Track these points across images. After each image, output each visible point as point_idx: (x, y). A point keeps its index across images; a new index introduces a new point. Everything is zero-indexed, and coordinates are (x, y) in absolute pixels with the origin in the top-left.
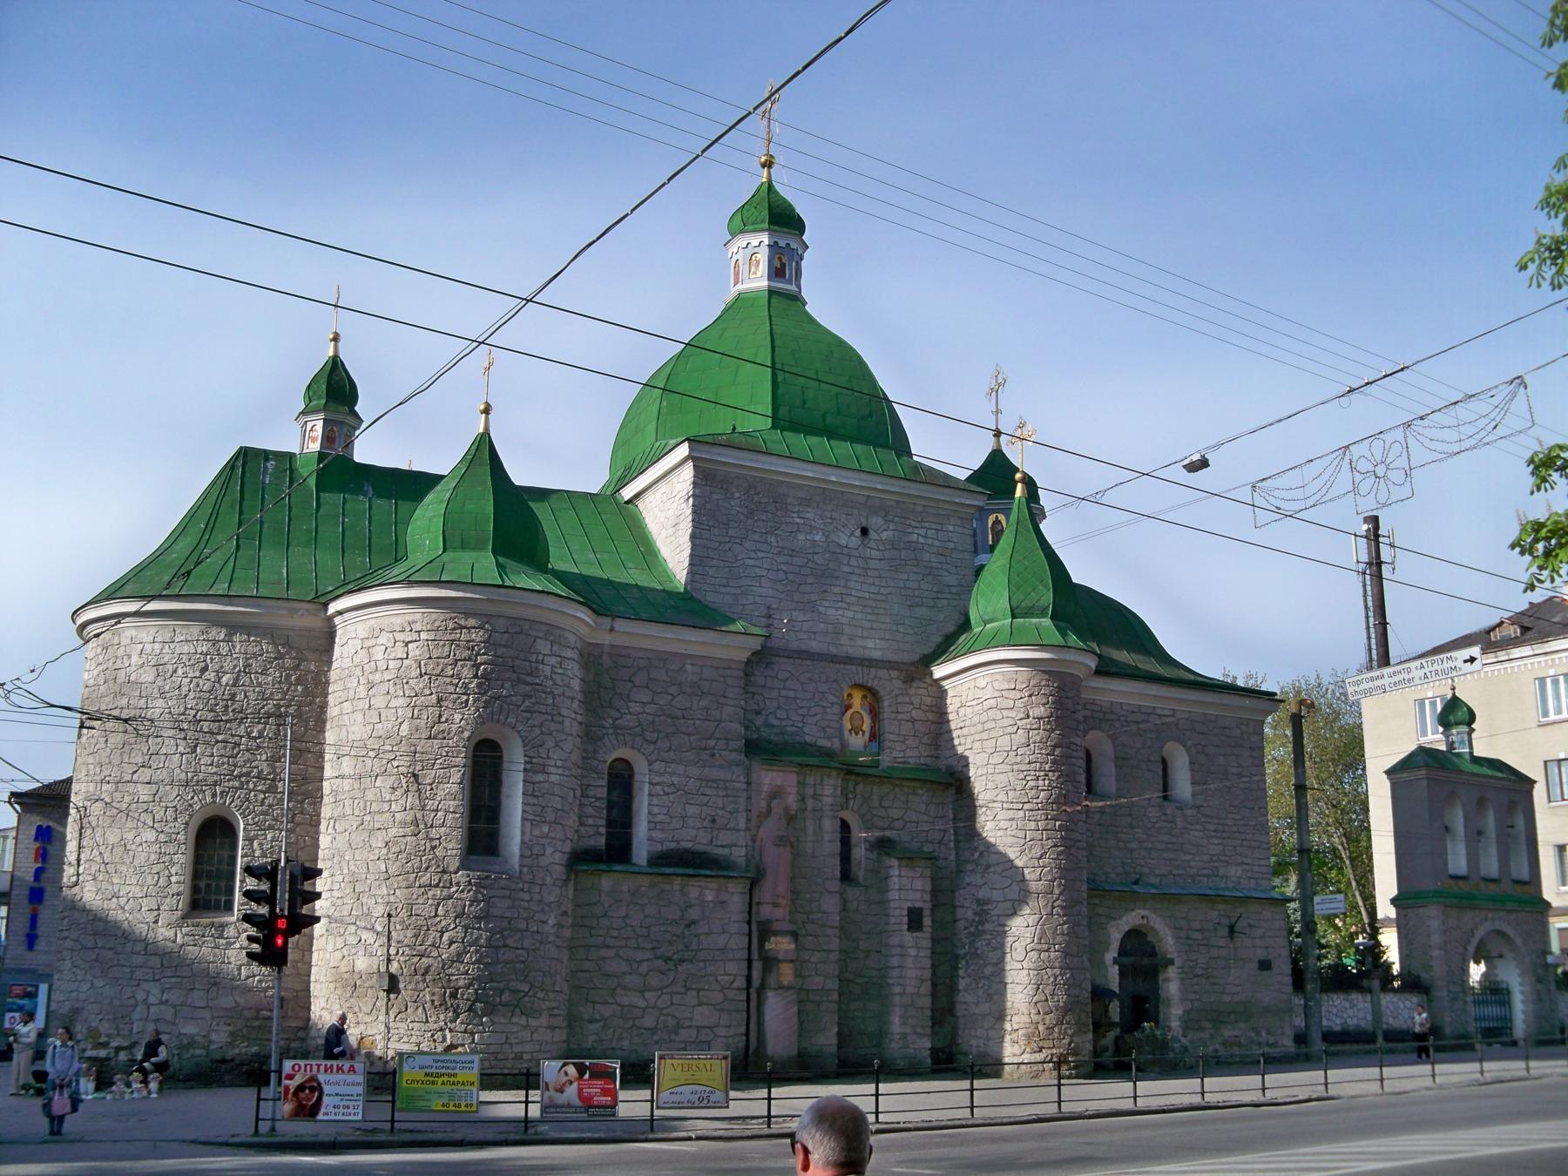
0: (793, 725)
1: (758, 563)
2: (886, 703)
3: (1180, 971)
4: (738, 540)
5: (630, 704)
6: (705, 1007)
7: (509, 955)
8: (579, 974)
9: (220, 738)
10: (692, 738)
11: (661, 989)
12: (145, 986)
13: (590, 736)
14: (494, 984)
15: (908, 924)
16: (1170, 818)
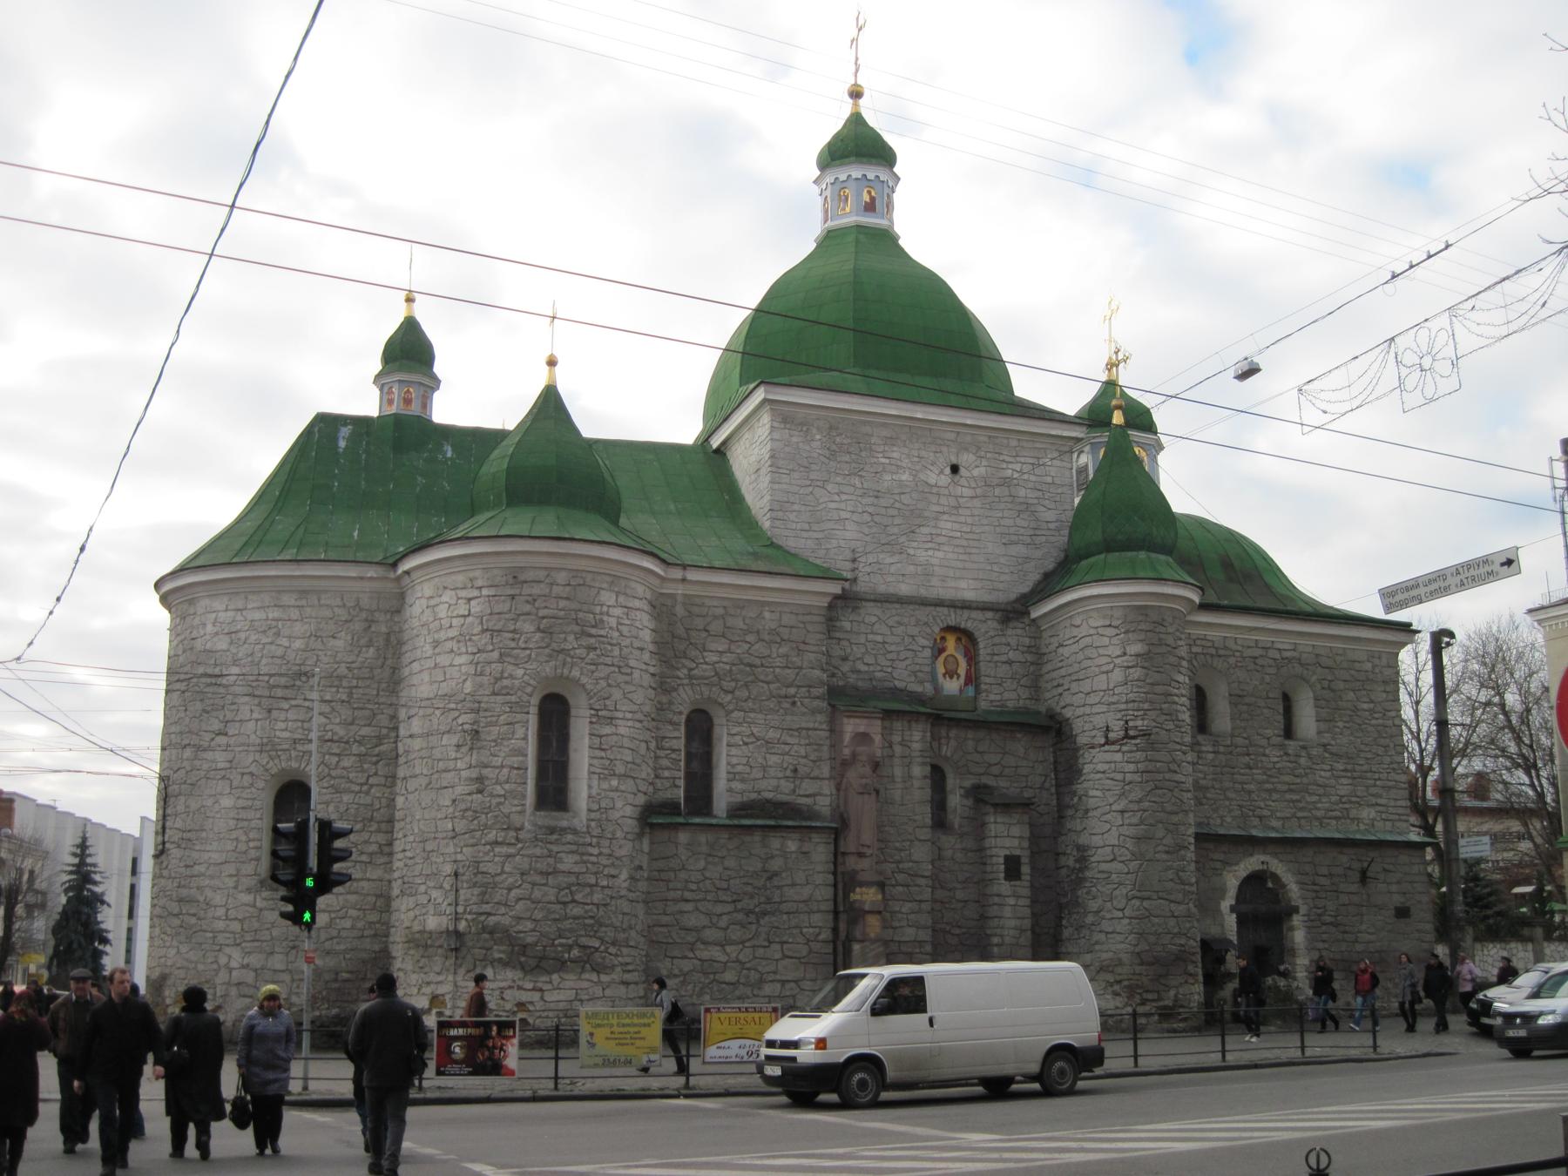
0: (881, 671)
1: (843, 506)
2: (981, 645)
3: (1306, 918)
4: (819, 483)
5: (705, 654)
6: (790, 960)
7: (577, 911)
8: (655, 929)
9: (293, 702)
10: (772, 686)
11: (743, 942)
12: (227, 950)
13: (663, 686)
14: (564, 941)
15: (1005, 872)
16: (1292, 759)
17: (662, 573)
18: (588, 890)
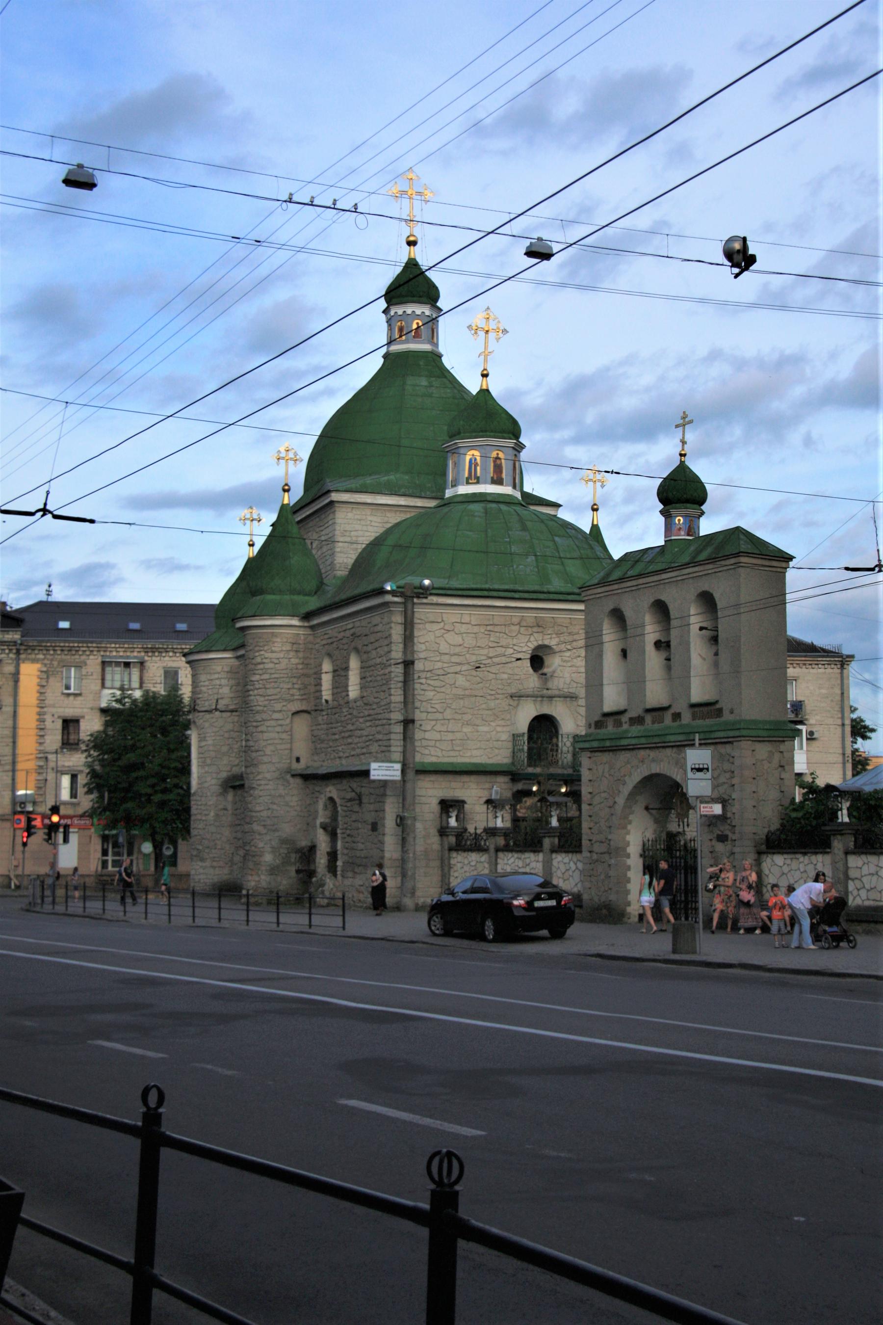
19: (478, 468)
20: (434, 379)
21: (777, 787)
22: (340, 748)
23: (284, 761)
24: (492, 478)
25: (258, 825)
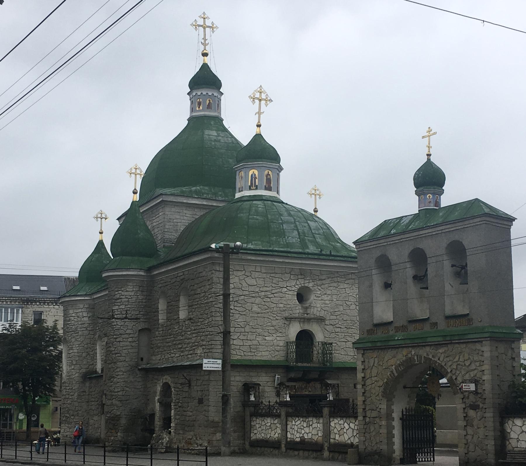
17: (90, 298)
18: (67, 399)
19: (257, 180)
20: (220, 132)
21: (511, 372)
22: (172, 351)
23: (133, 360)
24: (265, 186)
25: (116, 400)
